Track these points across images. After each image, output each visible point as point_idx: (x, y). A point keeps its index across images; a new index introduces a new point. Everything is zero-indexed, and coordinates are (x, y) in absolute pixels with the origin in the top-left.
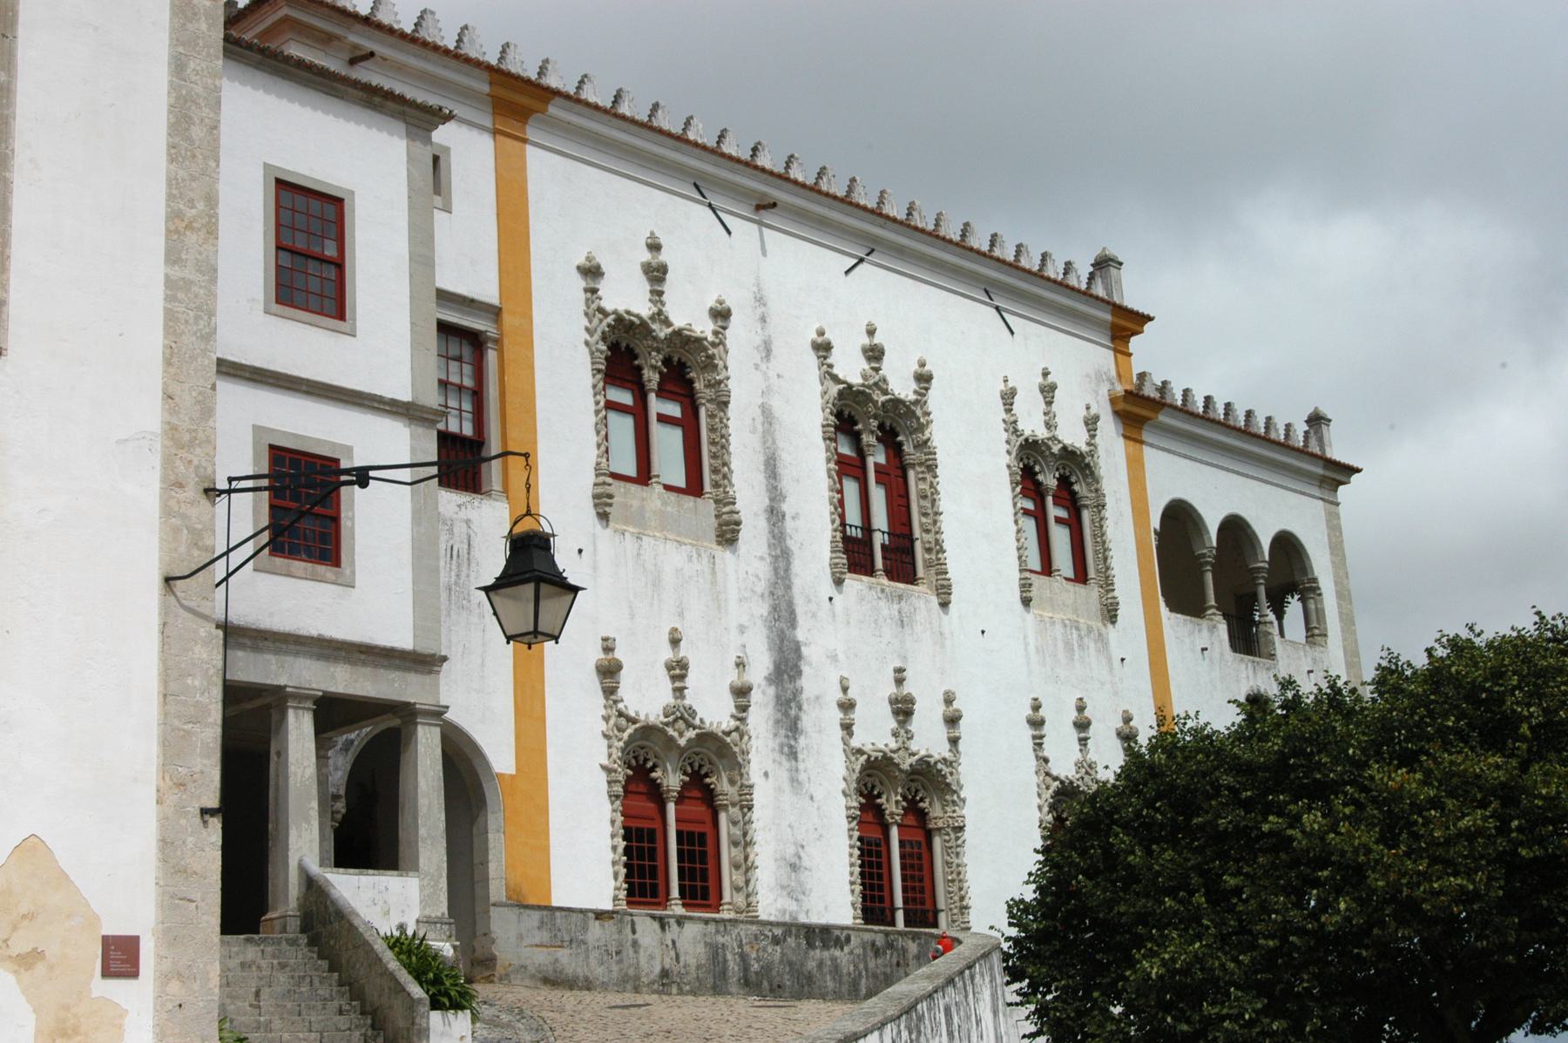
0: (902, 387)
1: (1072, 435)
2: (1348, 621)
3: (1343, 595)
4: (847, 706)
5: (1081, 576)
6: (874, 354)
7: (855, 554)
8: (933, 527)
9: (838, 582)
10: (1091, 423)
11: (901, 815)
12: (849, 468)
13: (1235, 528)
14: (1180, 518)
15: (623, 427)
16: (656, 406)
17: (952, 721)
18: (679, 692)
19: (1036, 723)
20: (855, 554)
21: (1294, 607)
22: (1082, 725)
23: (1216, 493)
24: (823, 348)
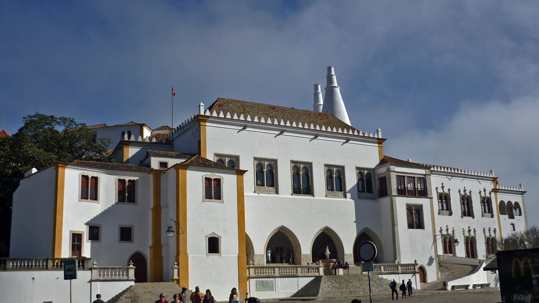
0: (468, 194)
1: (488, 195)
2: (525, 212)
3: (524, 209)
4: (464, 231)
5: (489, 212)
6: (465, 191)
7: (464, 214)
8: (472, 209)
9: (462, 217)
10: (490, 194)
11: (471, 243)
12: (463, 203)
13: (509, 202)
14: (502, 202)
15: (440, 204)
16: (444, 201)
17: (475, 231)
18: (447, 232)
19: (484, 230)
20: (464, 214)
21: (518, 210)
22: (489, 230)
23: (507, 198)
24: (459, 191)
